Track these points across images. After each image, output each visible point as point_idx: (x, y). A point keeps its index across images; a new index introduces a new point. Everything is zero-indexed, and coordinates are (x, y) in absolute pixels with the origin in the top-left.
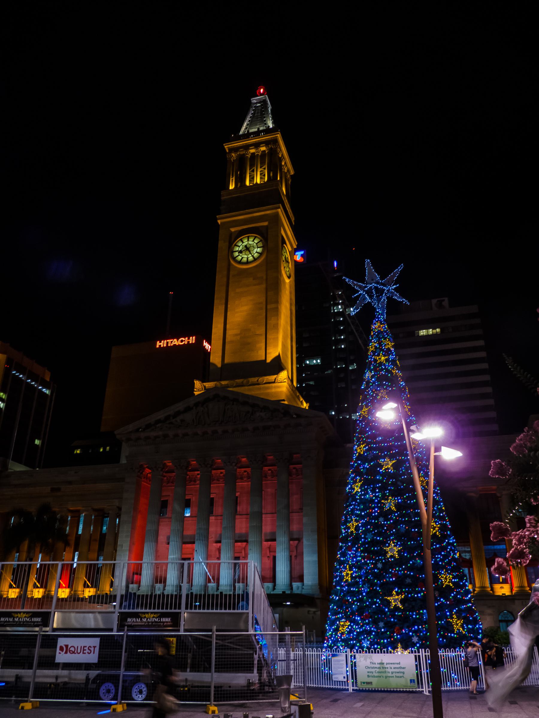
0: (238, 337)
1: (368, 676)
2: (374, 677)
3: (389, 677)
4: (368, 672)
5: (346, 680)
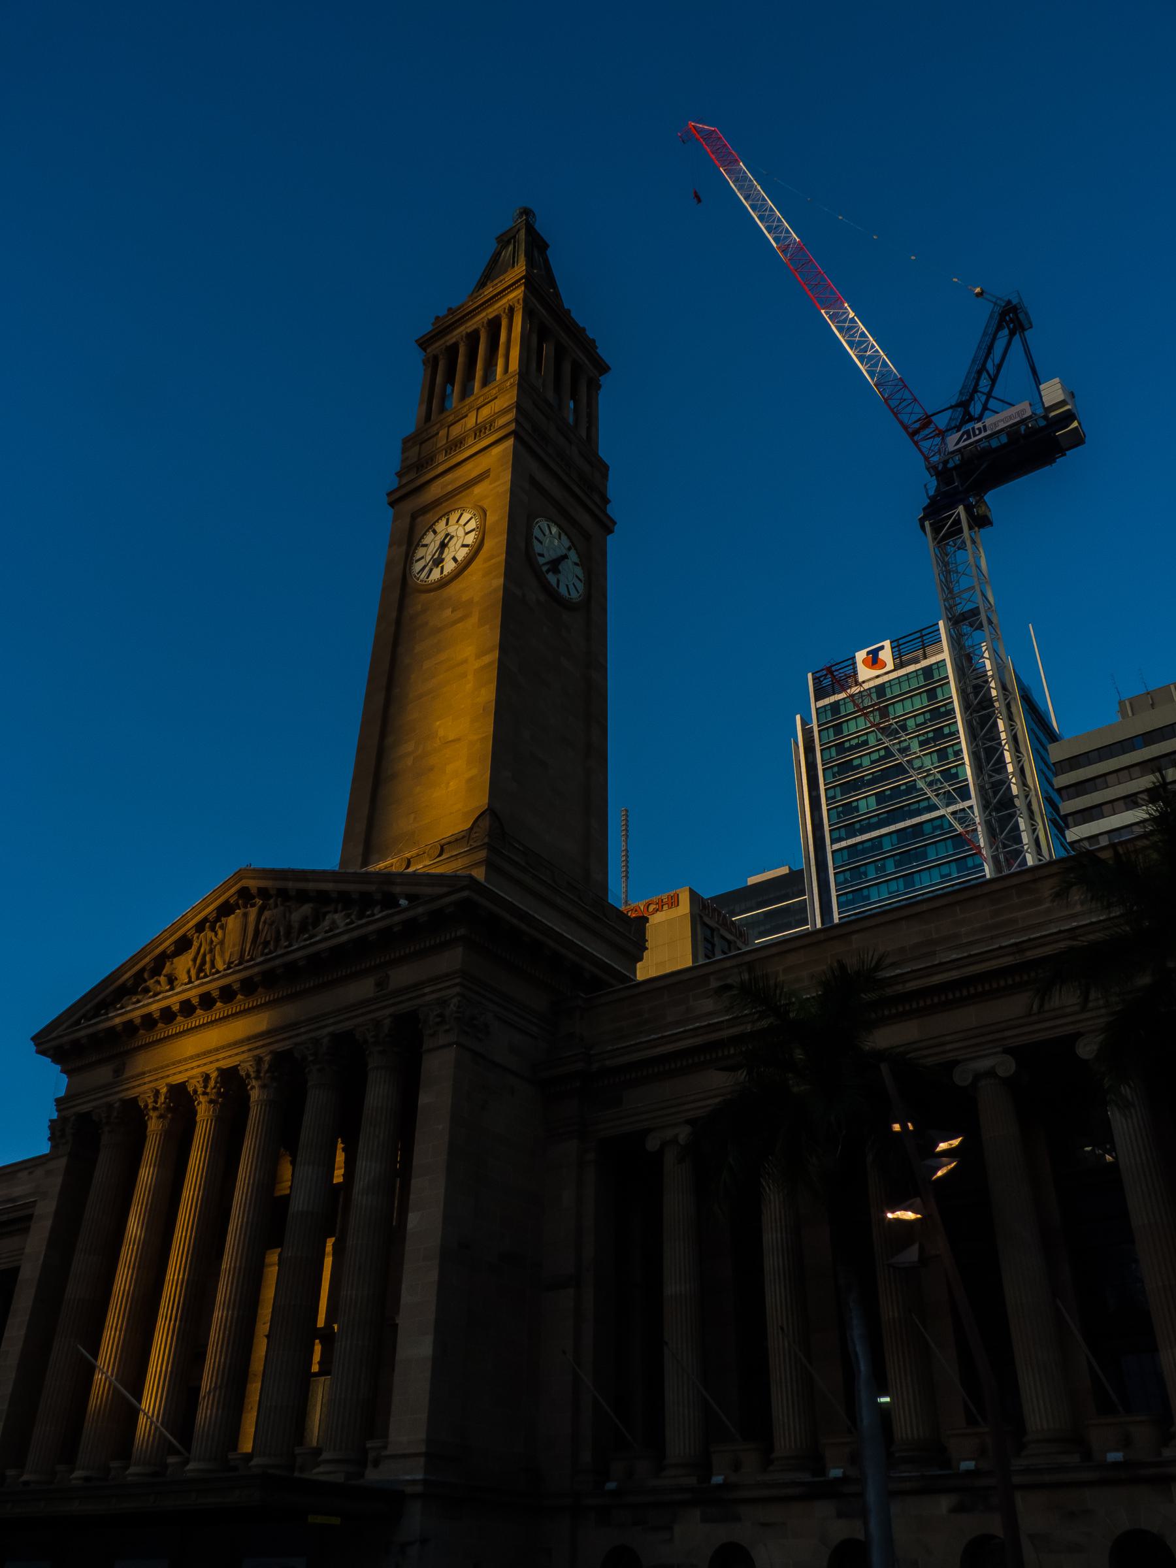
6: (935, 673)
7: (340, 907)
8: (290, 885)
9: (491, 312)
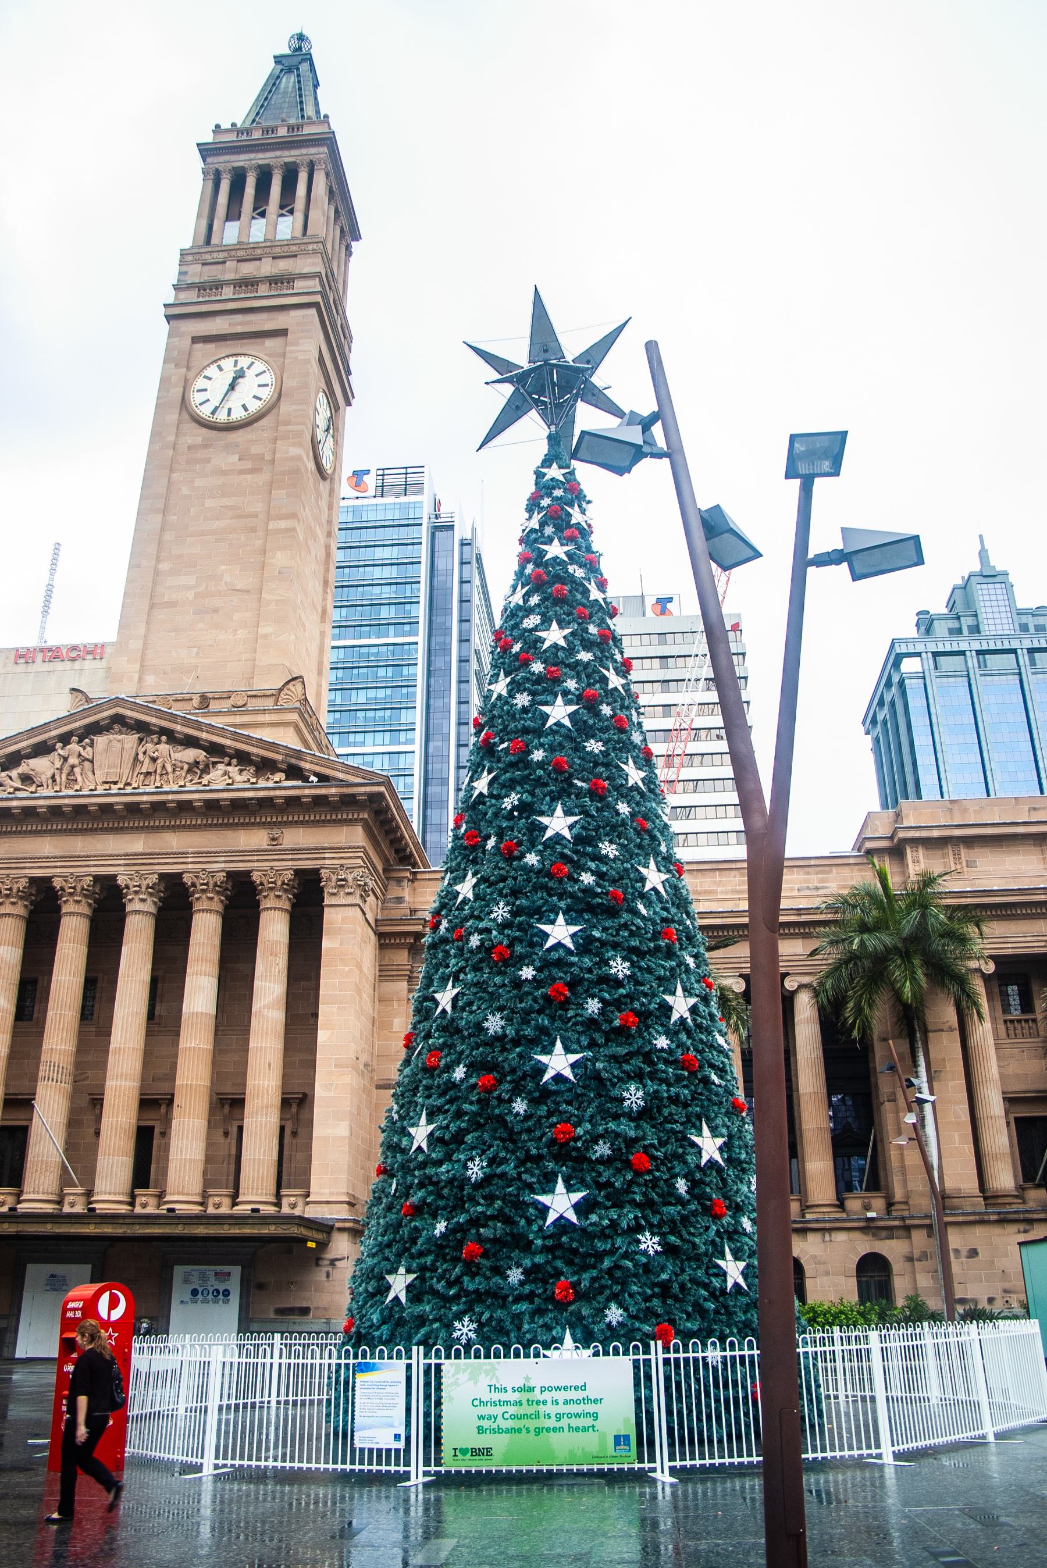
0: (190, 595)
1: (480, 1430)
2: (499, 1430)
3: (548, 1430)
4: (481, 1417)
5: (401, 1445)
6: (411, 511)
7: (234, 762)
8: (179, 728)
9: (290, 156)
